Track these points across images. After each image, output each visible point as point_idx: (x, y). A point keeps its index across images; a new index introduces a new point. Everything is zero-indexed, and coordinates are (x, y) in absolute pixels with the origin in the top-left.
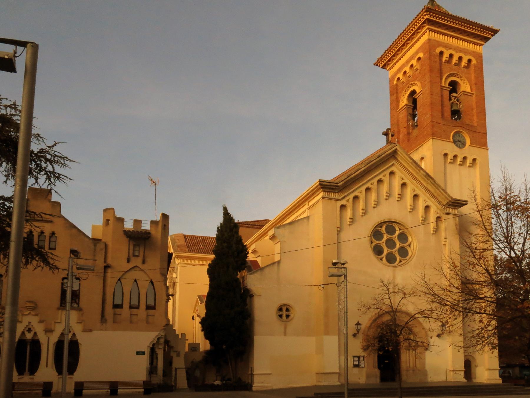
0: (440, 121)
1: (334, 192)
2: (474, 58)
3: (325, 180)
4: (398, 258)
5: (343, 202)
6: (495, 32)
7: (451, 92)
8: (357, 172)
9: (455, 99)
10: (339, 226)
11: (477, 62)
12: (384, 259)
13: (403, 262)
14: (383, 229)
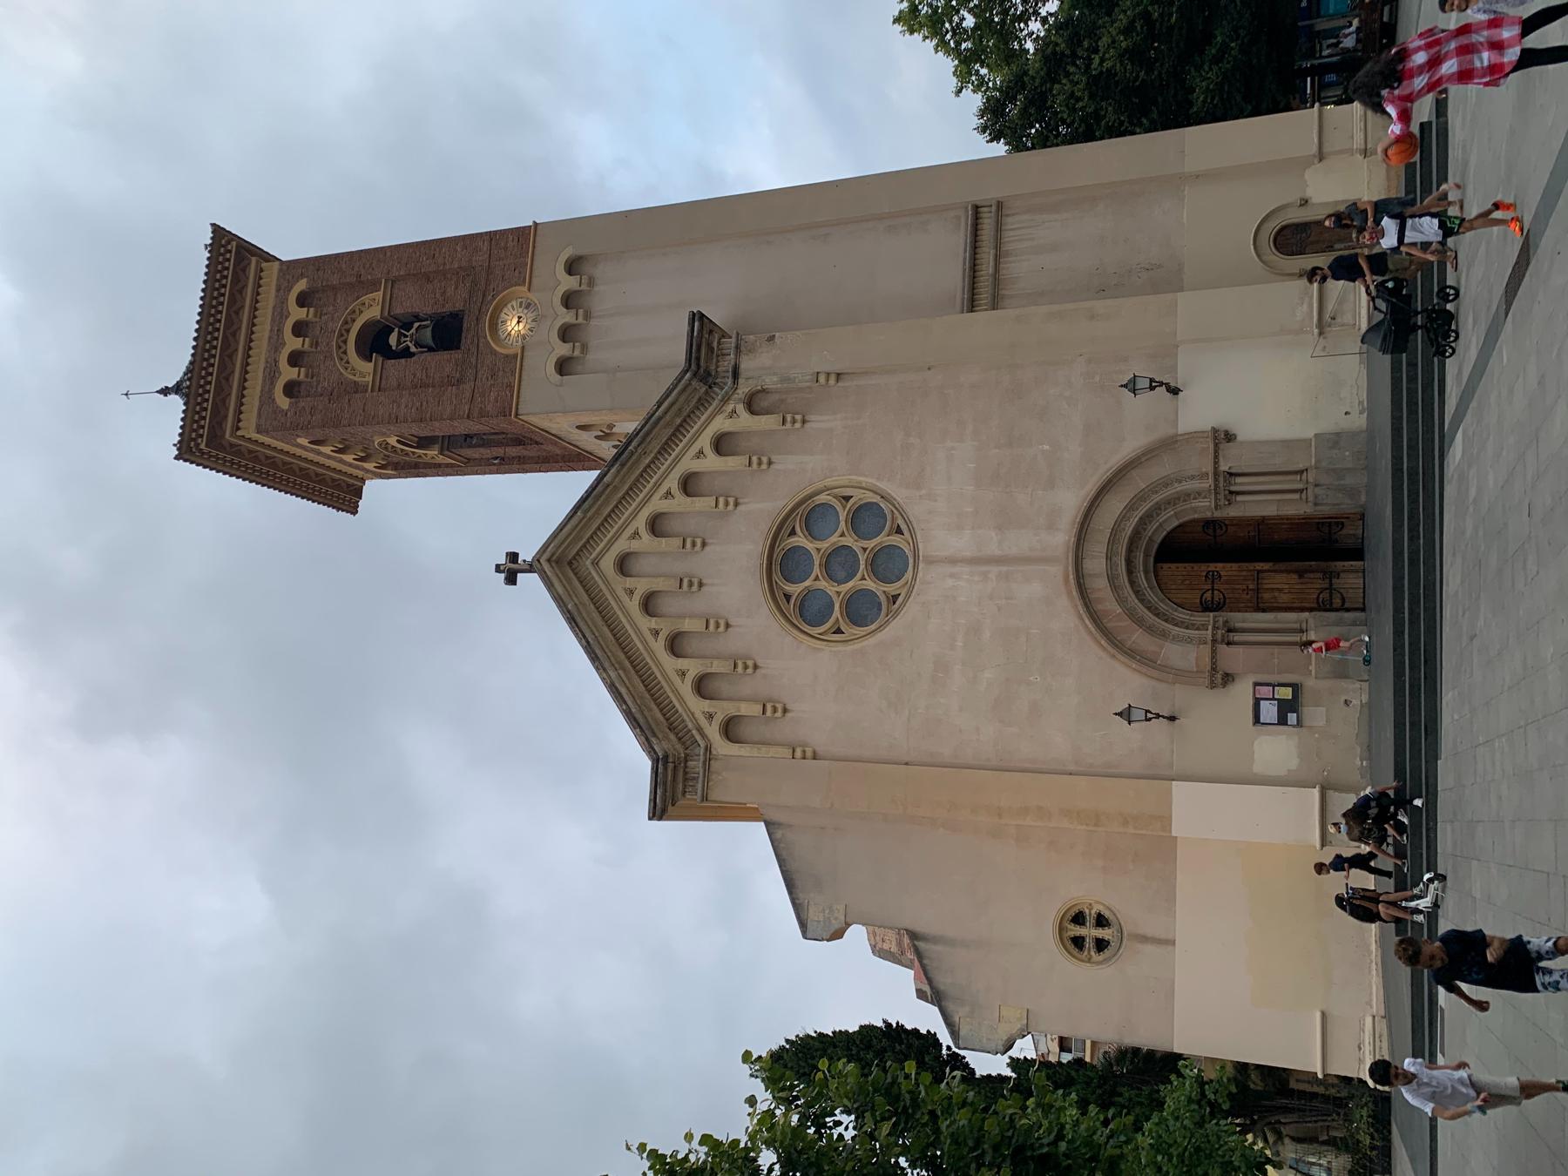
0: (467, 387)
1: (686, 761)
2: (292, 288)
3: (650, 800)
4: (883, 539)
5: (713, 731)
7: (389, 354)
8: (620, 694)
10: (787, 752)
11: (302, 276)
12: (892, 589)
13: (900, 521)
14: (795, 589)
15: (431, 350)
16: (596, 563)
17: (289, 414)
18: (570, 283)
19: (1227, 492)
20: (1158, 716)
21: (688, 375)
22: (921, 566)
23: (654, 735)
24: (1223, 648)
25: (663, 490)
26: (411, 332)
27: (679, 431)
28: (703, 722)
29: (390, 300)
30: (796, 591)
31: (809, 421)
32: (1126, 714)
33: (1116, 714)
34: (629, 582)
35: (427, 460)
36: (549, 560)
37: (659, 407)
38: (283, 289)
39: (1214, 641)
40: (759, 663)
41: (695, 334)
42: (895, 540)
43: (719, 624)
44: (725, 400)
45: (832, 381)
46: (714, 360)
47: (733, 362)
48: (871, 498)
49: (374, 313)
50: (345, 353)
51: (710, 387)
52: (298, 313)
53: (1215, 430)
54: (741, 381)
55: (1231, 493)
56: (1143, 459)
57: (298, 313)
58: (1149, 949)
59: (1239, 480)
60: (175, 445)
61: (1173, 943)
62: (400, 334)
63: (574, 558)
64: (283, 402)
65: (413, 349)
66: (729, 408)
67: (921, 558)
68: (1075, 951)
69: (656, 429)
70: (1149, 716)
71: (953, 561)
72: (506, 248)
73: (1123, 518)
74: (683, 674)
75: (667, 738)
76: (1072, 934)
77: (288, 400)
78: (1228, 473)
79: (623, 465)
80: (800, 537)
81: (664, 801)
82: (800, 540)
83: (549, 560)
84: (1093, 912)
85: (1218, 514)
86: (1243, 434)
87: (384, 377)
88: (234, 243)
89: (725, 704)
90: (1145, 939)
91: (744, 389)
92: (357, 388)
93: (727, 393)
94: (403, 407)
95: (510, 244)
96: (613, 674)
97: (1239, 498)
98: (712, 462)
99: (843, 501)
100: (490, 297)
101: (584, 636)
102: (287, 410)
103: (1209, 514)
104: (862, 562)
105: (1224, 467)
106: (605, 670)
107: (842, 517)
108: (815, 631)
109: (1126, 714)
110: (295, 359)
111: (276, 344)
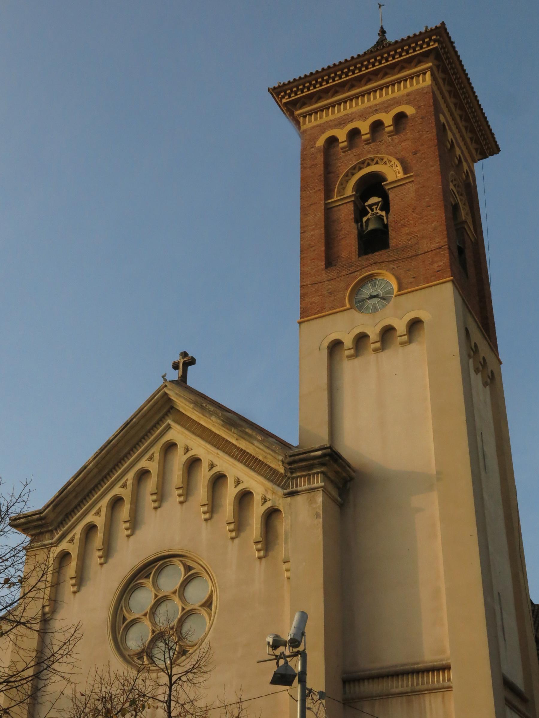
9: (376, 208)
17: (312, 149)
29: (399, 184)
31: (260, 562)
38: (409, 99)
46: (303, 473)
47: (299, 489)
49: (391, 178)
62: (377, 204)
72: (432, 263)
80: (185, 575)
83: (166, 394)
91: (282, 503)
94: (312, 233)
95: (436, 265)
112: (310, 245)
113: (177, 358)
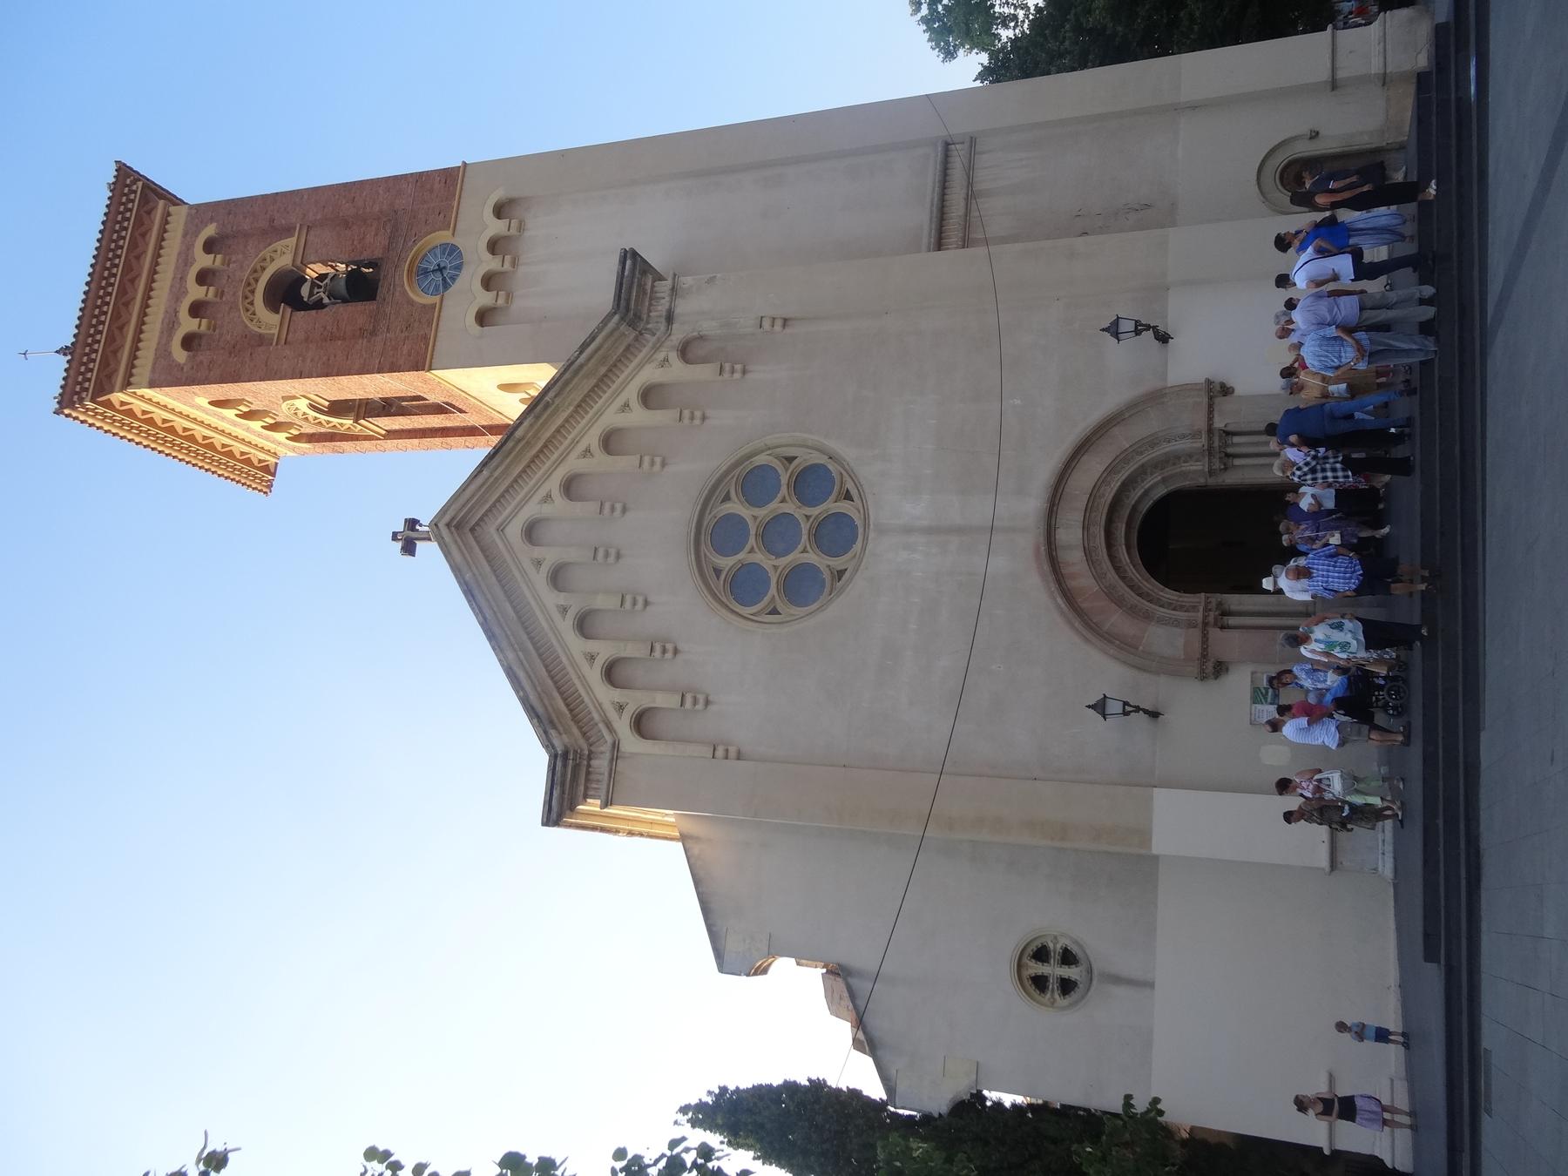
1: (590, 758)
2: (199, 232)
4: (831, 506)
5: (623, 726)
6: (123, 171)
9: (320, 287)
10: (708, 752)
11: (212, 220)
12: (837, 563)
13: (849, 485)
14: (727, 563)
15: (345, 301)
16: (501, 529)
17: (185, 370)
18: (496, 227)
19: (1223, 455)
20: (1138, 709)
21: (617, 317)
22: (872, 535)
23: (555, 727)
24: (1215, 633)
25: (581, 447)
26: (325, 282)
27: (602, 382)
28: (612, 714)
30: (727, 565)
31: (750, 372)
32: (1100, 707)
33: (1089, 707)
34: (537, 552)
35: (342, 430)
36: (448, 525)
37: (581, 353)
38: (190, 233)
39: (1205, 624)
40: (680, 647)
41: (626, 274)
42: (844, 507)
43: (635, 600)
44: (656, 348)
45: (778, 328)
47: (667, 306)
48: (817, 458)
50: (252, 303)
51: (641, 334)
52: (203, 260)
53: (1209, 382)
54: (675, 326)
55: (1227, 455)
56: (1127, 415)
57: (203, 260)
58: (1121, 991)
59: (1236, 439)
60: (55, 398)
61: (1150, 985)
63: (477, 524)
64: (180, 355)
65: (326, 300)
66: (661, 356)
67: (872, 527)
68: (1036, 994)
69: (576, 380)
70: (1128, 709)
71: (908, 530)
72: (431, 191)
73: (1103, 481)
74: (591, 658)
75: (568, 732)
76: (1032, 972)
77: (185, 353)
78: (1224, 431)
79: (537, 417)
80: (735, 503)
81: (561, 804)
82: (736, 507)
83: (448, 525)
84: (1059, 946)
85: (1212, 481)
86: (1240, 390)
87: (291, 328)
88: (140, 184)
89: (638, 694)
90: (1117, 980)
91: (679, 333)
92: (262, 340)
93: (659, 339)
94: (309, 360)
95: (437, 186)
96: (511, 655)
97: (1237, 462)
98: (639, 416)
99: (786, 462)
100: (411, 243)
101: (481, 612)
102: (184, 364)
103: (1202, 481)
104: (805, 532)
105: (1219, 423)
106: (502, 651)
107: (784, 479)
108: (747, 611)
109: (1100, 707)
110: (196, 310)
111: (178, 293)
112: (324, 363)
113: (400, 527)
